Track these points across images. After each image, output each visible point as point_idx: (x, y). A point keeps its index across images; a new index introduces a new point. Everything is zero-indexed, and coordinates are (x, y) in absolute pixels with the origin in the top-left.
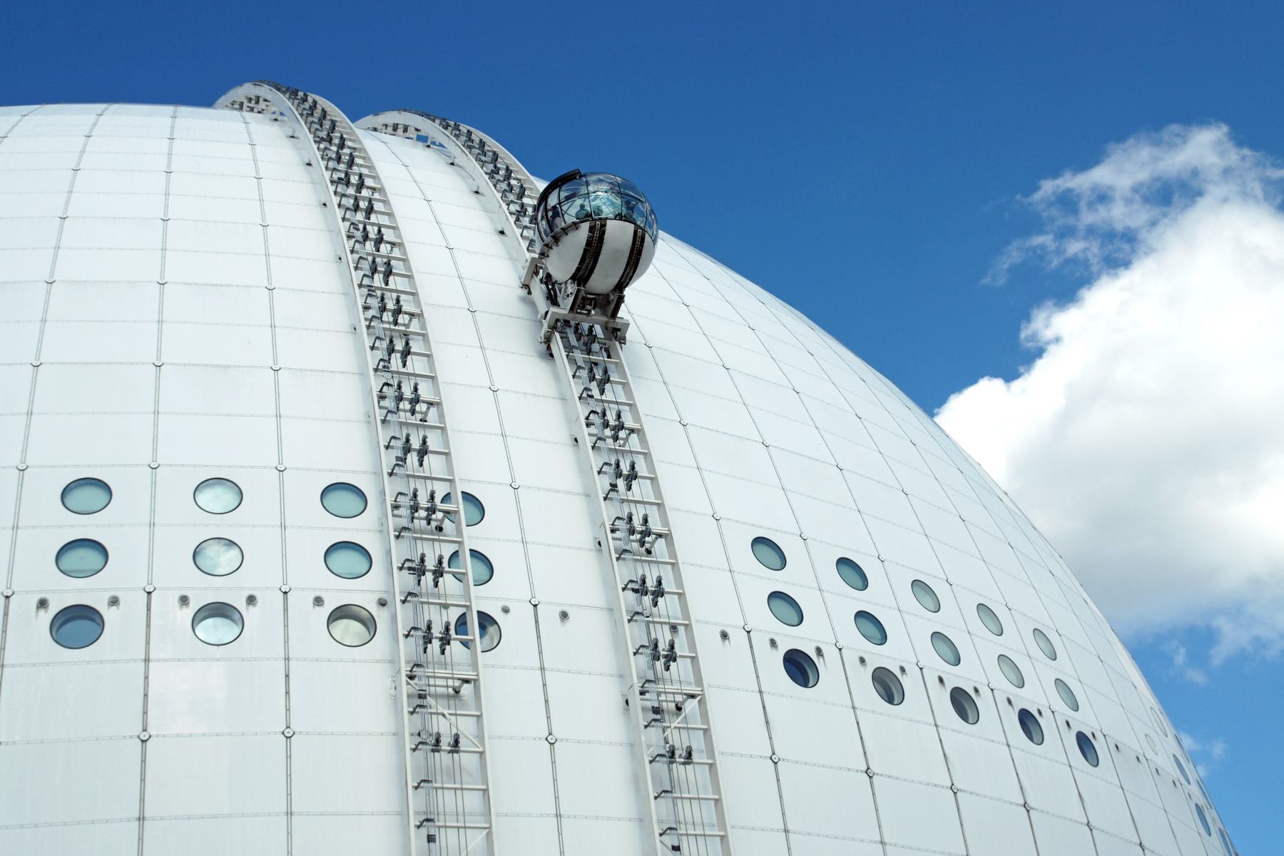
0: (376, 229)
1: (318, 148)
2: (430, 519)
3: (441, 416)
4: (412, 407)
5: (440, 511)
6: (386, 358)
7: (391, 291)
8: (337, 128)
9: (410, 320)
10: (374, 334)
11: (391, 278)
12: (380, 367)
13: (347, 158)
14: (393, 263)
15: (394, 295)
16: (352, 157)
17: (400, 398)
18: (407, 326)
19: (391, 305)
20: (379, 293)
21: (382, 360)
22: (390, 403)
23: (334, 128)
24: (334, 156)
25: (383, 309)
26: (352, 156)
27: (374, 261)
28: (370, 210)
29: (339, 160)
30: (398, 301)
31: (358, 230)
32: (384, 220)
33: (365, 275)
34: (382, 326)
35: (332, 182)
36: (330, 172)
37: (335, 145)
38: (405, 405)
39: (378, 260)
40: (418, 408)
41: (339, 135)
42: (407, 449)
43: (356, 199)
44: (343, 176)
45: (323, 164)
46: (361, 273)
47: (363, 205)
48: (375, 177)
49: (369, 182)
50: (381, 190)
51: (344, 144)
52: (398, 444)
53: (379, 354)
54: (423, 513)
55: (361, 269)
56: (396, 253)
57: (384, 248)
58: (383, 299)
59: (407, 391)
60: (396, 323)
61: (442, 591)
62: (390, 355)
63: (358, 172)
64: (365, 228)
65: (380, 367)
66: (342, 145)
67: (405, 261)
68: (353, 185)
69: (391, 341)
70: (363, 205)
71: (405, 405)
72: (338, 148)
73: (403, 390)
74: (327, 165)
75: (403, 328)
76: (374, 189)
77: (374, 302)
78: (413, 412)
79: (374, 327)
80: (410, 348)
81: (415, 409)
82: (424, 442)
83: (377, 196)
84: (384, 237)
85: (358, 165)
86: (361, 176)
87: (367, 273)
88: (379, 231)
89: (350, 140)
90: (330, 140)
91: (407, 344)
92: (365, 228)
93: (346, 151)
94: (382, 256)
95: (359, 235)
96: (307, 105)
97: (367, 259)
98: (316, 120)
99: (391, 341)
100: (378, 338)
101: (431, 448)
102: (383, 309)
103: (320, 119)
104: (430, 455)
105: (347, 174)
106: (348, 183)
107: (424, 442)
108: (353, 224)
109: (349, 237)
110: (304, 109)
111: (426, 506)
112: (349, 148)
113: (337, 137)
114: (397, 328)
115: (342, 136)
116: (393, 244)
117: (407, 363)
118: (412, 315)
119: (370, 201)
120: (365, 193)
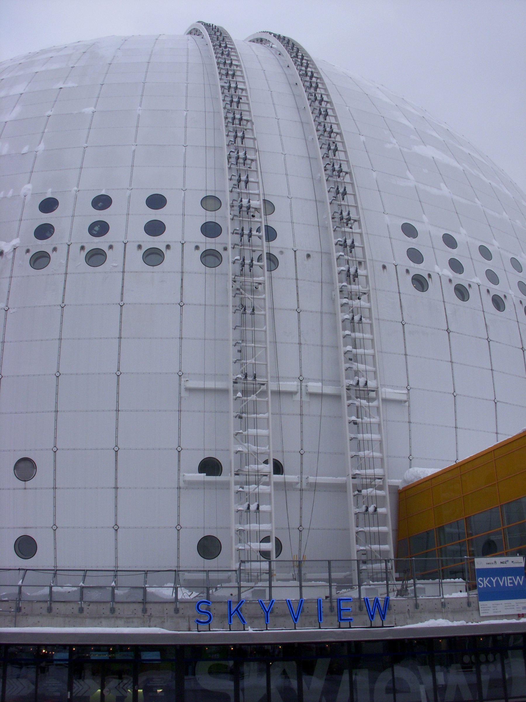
0: (320, 95)
1: (293, 60)
2: (348, 223)
3: (351, 178)
4: (338, 174)
5: (352, 220)
6: (327, 153)
7: (328, 123)
8: (299, 51)
9: (336, 135)
10: (322, 142)
11: (327, 117)
12: (325, 156)
13: (305, 64)
14: (328, 110)
15: (329, 125)
16: (308, 64)
17: (334, 170)
18: (335, 138)
19: (328, 129)
20: (323, 124)
21: (325, 153)
22: (329, 172)
23: (298, 51)
24: (300, 64)
25: (325, 131)
26: (308, 64)
27: (320, 110)
28: (317, 87)
29: (302, 65)
30: (331, 127)
31: (312, 96)
32: (323, 92)
33: (316, 116)
34: (324, 138)
35: (300, 75)
36: (299, 71)
37: (299, 59)
38: (335, 173)
39: (322, 110)
40: (341, 174)
41: (301, 54)
42: (338, 192)
43: (311, 82)
44: (304, 72)
45: (295, 67)
46: (315, 115)
47: (314, 85)
48: (318, 73)
49: (315, 75)
50: (321, 79)
51: (303, 58)
52: (334, 190)
53: (325, 151)
54: (345, 221)
55: (315, 113)
56: (329, 106)
57: (323, 104)
58: (324, 126)
59: (337, 167)
60: (330, 137)
61: (354, 255)
62: (328, 151)
63: (311, 70)
64: (315, 95)
65: (325, 156)
66: (302, 59)
67: (333, 110)
68: (309, 76)
69: (329, 145)
70: (314, 85)
71: (335, 173)
72: (301, 60)
73: (335, 166)
74: (297, 67)
75: (333, 139)
76: (317, 78)
77: (321, 128)
78: (339, 177)
79: (321, 139)
80: (337, 148)
81: (340, 175)
82: (345, 189)
83: (318, 81)
84: (324, 99)
85: (310, 68)
86: (312, 72)
87: (317, 115)
88: (321, 96)
89: (306, 57)
90: (297, 56)
91: (336, 146)
92: (315, 95)
93: (304, 61)
94: (323, 108)
95: (313, 98)
96: (286, 42)
97: (317, 109)
98: (291, 48)
99: (329, 145)
100: (323, 144)
101: (348, 192)
102: (325, 131)
103: (292, 48)
104: (347, 195)
105: (306, 71)
106: (307, 75)
107: (345, 189)
108: (310, 93)
109: (309, 99)
110: (285, 43)
111: (346, 218)
112: (305, 60)
113: (300, 55)
114: (331, 139)
115: (302, 55)
116: (327, 102)
117: (336, 154)
118: (337, 134)
119: (317, 83)
120: (314, 79)
